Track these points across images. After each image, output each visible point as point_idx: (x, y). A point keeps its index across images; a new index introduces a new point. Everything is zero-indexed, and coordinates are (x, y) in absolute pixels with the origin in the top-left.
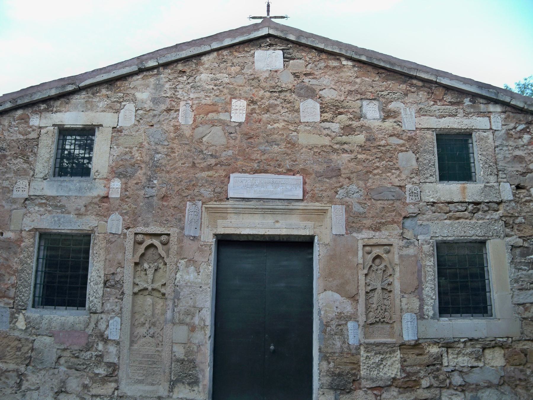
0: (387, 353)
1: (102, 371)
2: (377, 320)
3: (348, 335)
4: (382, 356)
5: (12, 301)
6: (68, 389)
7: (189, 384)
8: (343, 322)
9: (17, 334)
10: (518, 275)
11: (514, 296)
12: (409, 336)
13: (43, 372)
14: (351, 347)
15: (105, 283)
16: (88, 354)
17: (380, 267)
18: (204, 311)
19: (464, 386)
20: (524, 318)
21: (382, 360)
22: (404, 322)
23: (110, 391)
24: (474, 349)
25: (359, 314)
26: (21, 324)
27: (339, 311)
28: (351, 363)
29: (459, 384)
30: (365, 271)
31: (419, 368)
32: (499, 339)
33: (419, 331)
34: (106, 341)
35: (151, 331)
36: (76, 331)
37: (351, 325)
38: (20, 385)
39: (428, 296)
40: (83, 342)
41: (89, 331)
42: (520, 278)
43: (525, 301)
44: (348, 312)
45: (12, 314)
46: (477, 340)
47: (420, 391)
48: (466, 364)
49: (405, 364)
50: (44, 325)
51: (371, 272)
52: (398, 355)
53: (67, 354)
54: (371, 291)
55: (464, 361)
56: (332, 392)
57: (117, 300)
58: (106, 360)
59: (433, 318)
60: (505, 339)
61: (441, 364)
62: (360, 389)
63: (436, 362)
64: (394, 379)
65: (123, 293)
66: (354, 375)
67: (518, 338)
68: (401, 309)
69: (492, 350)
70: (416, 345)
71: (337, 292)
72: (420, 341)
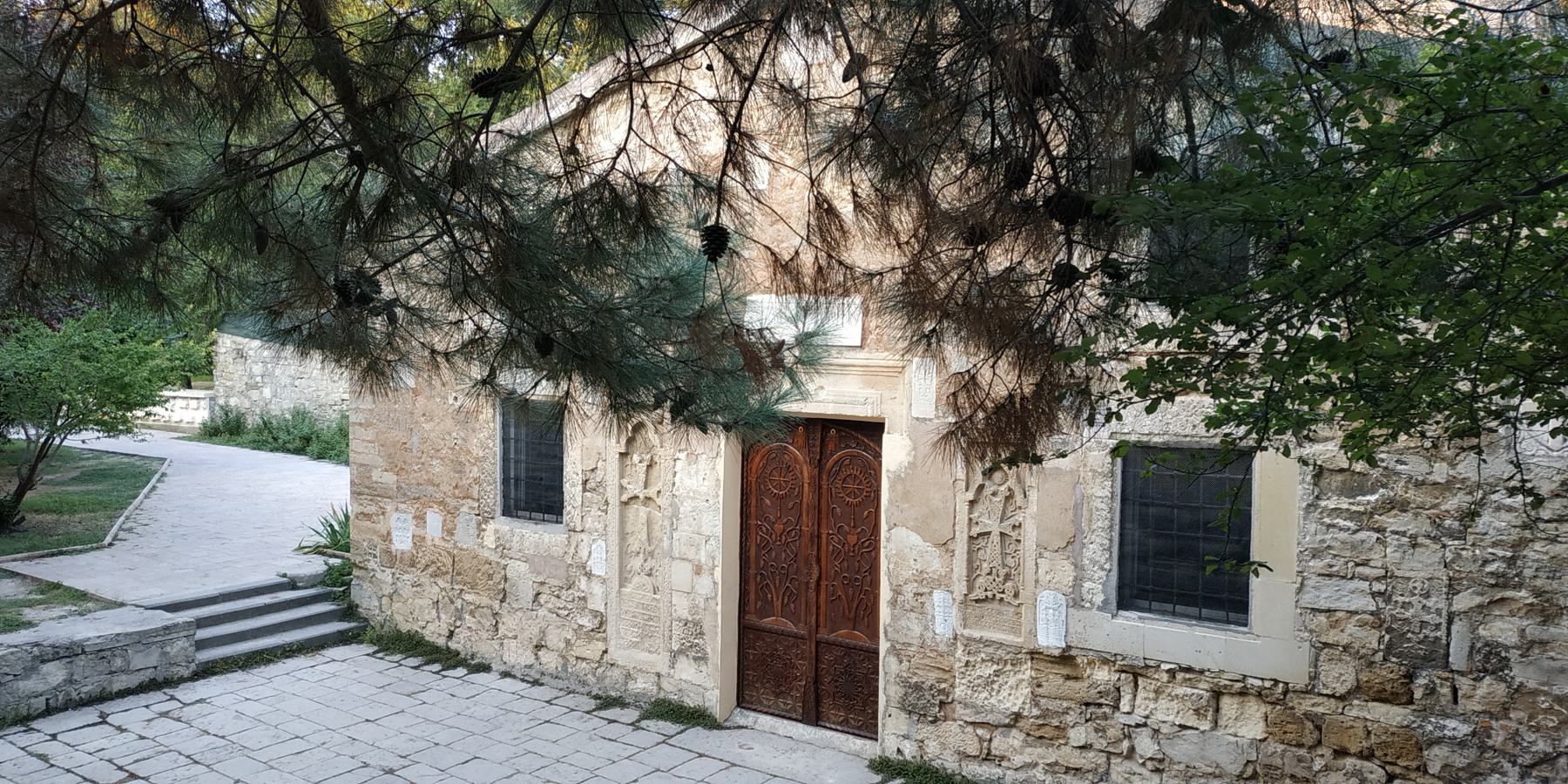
0: (1006, 661)
1: (587, 622)
2: (989, 594)
3: (933, 616)
4: (995, 667)
5: (476, 505)
7: (695, 659)
8: (925, 590)
9: (486, 554)
10: (1323, 541)
11: (1306, 589)
12: (1050, 639)
13: (519, 614)
14: (938, 639)
15: (585, 482)
17: (1002, 488)
18: (712, 542)
19: (1161, 761)
20: (1326, 645)
21: (997, 673)
22: (1041, 607)
24: (1190, 691)
25: (955, 579)
26: (490, 541)
27: (918, 566)
28: (939, 669)
29: (1149, 756)
30: (970, 495)
31: (1065, 704)
32: (1251, 681)
33: (1070, 630)
34: (589, 575)
35: (647, 566)
36: (553, 557)
37: (938, 596)
39: (1094, 563)
42: (1329, 547)
43: (1333, 606)
44: (934, 572)
45: (479, 524)
46: (1202, 672)
47: (1066, 750)
48: (1171, 718)
49: (1040, 691)
50: (515, 546)
51: (982, 499)
52: (1027, 672)
53: (545, 589)
54: (980, 535)
55: (1166, 712)
56: (904, 715)
57: (599, 513)
58: (590, 606)
59: (1099, 609)
60: (1268, 684)
61: (1116, 708)
62: (955, 720)
63: (1102, 701)
64: (1017, 716)
65: (607, 503)
66: (941, 691)
67: (1300, 686)
68: (1037, 581)
69: (1236, 700)
70: (1065, 658)
71: (917, 530)
72: (1073, 652)
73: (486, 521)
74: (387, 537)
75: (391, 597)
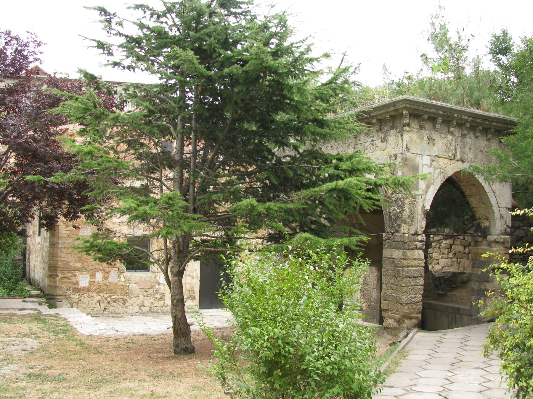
1: (158, 296)
6: (145, 305)
9: (121, 283)
16: (151, 290)
23: (162, 304)
26: (123, 279)
34: (159, 284)
38: (124, 304)
40: (150, 285)
41: (152, 281)
50: (133, 279)
73: (121, 273)
74: (77, 283)
75: (77, 303)
